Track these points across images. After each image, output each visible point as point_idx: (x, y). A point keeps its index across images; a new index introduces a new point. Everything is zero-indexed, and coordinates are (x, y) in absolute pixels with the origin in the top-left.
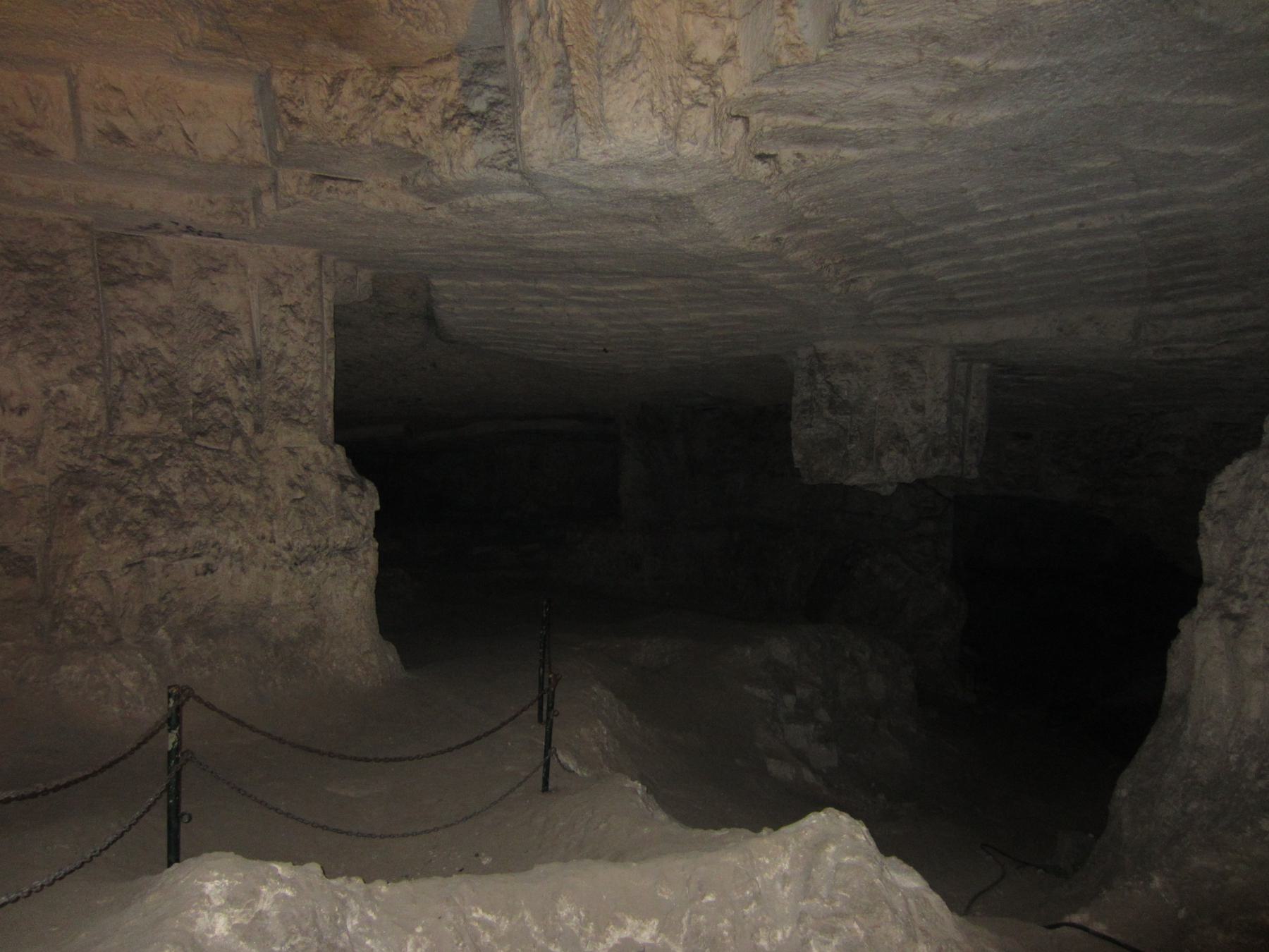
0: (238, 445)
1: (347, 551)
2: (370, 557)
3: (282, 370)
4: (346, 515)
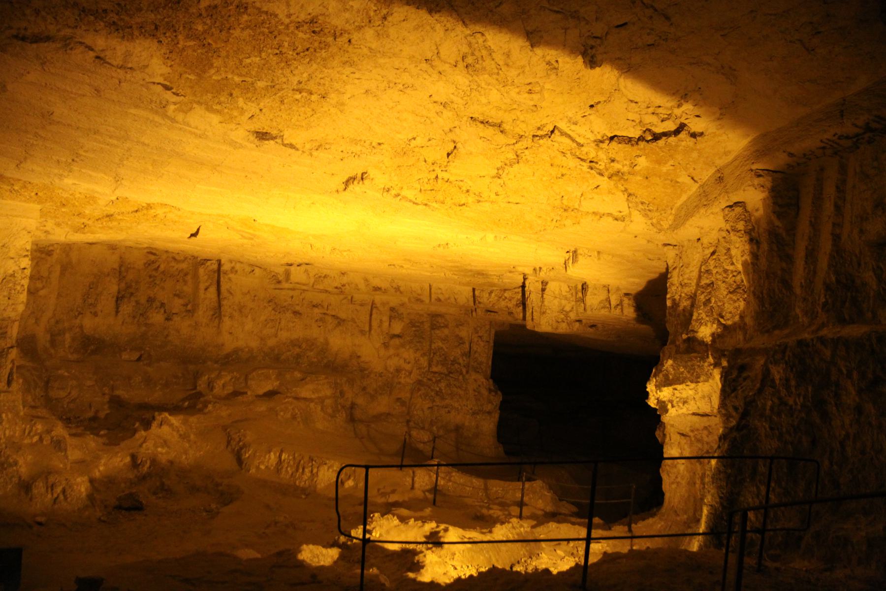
0: (461, 377)
1: (489, 413)
2: (496, 416)
3: (476, 355)
4: (490, 402)
